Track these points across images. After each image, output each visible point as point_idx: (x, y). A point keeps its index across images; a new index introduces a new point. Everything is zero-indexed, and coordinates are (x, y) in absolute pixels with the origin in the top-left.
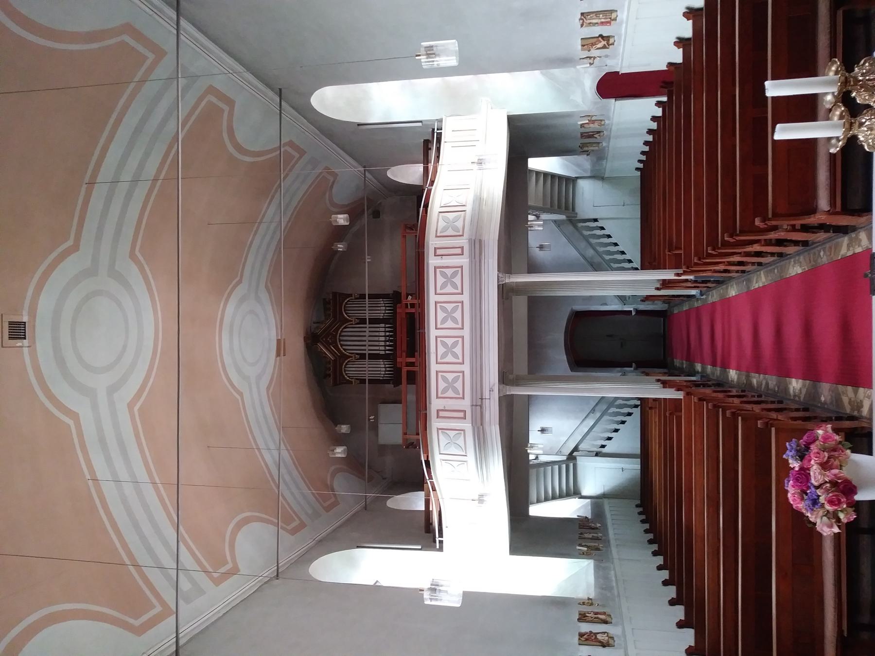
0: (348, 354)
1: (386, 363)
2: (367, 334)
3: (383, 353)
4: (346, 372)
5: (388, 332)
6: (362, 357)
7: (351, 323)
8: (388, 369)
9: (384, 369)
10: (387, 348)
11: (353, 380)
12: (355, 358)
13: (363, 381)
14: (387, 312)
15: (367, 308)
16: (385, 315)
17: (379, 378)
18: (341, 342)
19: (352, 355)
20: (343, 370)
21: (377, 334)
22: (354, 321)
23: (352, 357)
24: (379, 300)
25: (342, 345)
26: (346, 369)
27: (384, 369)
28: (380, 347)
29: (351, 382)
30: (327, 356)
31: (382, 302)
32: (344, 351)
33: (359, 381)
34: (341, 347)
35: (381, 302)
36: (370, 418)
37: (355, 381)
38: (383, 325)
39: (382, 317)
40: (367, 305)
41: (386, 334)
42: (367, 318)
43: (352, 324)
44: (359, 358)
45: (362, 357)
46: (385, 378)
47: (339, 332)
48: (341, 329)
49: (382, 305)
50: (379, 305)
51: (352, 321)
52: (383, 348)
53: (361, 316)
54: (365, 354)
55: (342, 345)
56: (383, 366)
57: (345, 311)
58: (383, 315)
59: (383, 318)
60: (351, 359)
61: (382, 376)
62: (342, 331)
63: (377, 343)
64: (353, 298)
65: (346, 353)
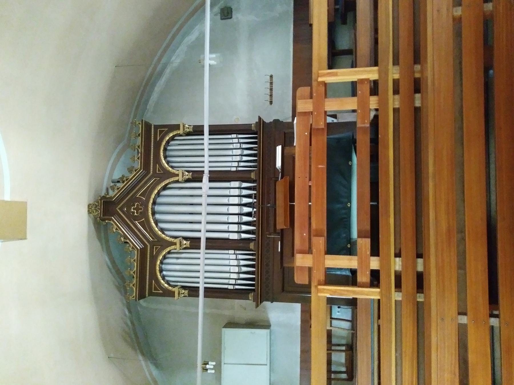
0: (168, 238)
1: (240, 257)
2: (203, 200)
3: (234, 236)
4: (164, 273)
5: (245, 205)
6: (195, 243)
7: (176, 179)
9: (236, 269)
10: (244, 228)
11: (176, 290)
12: (181, 246)
13: (193, 291)
14: (245, 158)
15: (206, 153)
16: (242, 164)
18: (157, 216)
19: (177, 241)
20: (158, 268)
21: (225, 200)
22: (181, 175)
23: (175, 244)
24: (229, 136)
25: (156, 222)
26: (164, 266)
27: (236, 269)
28: (231, 226)
29: (171, 294)
30: (128, 241)
31: (236, 141)
32: (160, 233)
33: (186, 292)
34: (157, 225)
35: (234, 139)
36: (208, 366)
37: (179, 294)
38: (236, 184)
39: (234, 169)
40: (206, 147)
41: (241, 200)
42: (206, 170)
43: (177, 182)
44: (189, 246)
45: (195, 243)
47: (153, 196)
48: (156, 191)
49: (235, 146)
50: (231, 146)
51: (178, 175)
52: (235, 228)
53: (195, 167)
54: (199, 239)
55: (156, 222)
56: (235, 263)
57: (165, 157)
58: (236, 164)
59: (237, 171)
60: (173, 247)
61: (233, 282)
62: (158, 195)
63: (224, 218)
64: (181, 132)
65: (163, 236)
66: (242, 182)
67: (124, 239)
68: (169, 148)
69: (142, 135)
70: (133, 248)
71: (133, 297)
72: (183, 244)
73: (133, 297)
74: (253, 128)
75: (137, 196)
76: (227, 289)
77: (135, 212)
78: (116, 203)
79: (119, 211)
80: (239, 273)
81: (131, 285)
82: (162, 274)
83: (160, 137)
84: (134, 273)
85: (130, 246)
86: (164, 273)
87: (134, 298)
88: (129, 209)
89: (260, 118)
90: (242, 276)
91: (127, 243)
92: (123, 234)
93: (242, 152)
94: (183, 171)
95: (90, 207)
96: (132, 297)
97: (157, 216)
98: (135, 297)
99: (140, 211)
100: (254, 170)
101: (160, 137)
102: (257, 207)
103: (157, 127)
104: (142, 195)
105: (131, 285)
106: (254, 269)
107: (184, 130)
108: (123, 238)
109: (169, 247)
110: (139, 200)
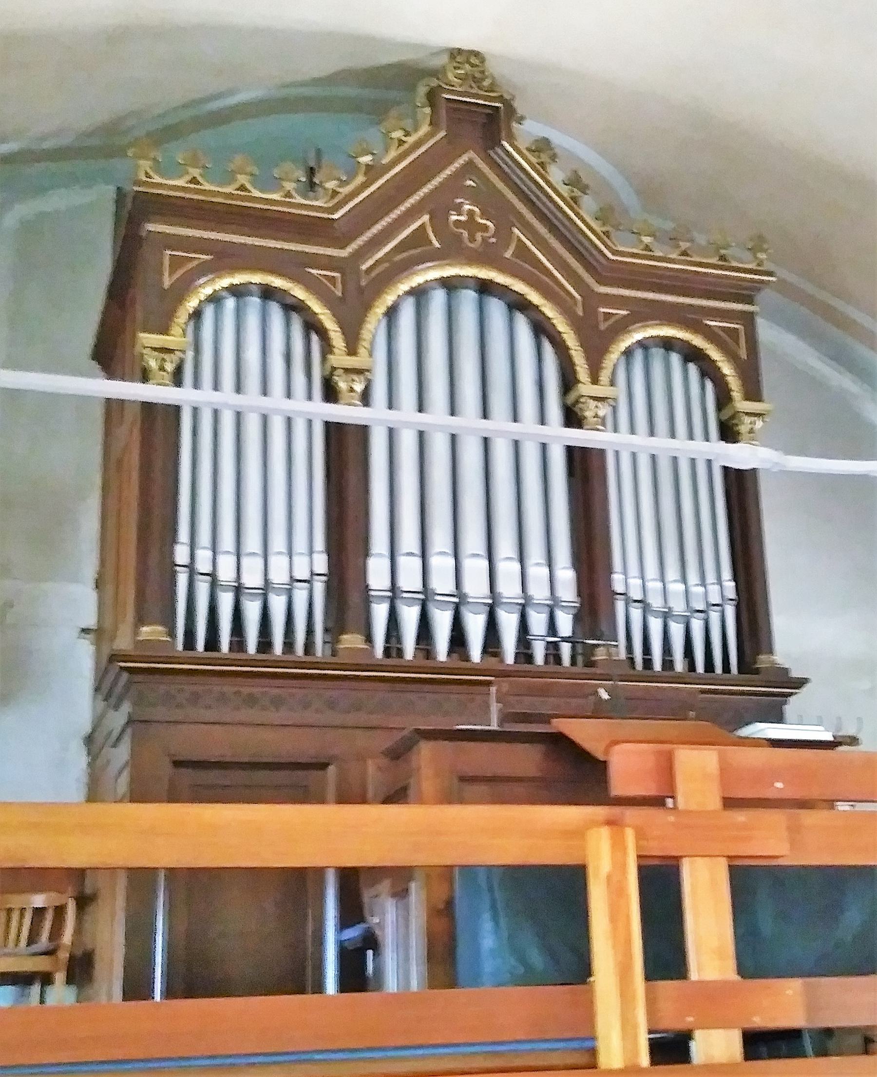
4: (230, 303)
8: (252, 611)
10: (410, 616)
11: (175, 339)
17: (183, 534)
18: (438, 297)
34: (412, 292)
38: (568, 592)
46: (182, 580)
52: (410, 580)
56: (279, 576)
63: (440, 539)
66: (574, 611)
67: (367, 165)
68: (675, 359)
69: (721, 268)
70: (335, 193)
71: (146, 173)
72: (164, 360)
73: (146, 173)
74: (763, 661)
75: (516, 231)
76: (174, 540)
77: (463, 218)
78: (491, 153)
79: (461, 161)
80: (238, 590)
81: (195, 172)
82: (224, 294)
83: (721, 333)
84: (242, 188)
85: (343, 183)
86: (230, 303)
87: (144, 179)
88: (474, 196)
89: (800, 683)
90: (226, 602)
91: (352, 176)
92: (384, 161)
93: (678, 618)
94: (615, 399)
95: (473, 60)
96: (149, 171)
97: (438, 297)
98: (148, 180)
99: (465, 234)
100: (172, 633)
101: (721, 333)
102: (485, 666)
103: (748, 319)
104: (522, 251)
105: (195, 172)
106: (510, 658)
107: (747, 414)
108: (370, 163)
109: (338, 329)
110: (503, 233)
